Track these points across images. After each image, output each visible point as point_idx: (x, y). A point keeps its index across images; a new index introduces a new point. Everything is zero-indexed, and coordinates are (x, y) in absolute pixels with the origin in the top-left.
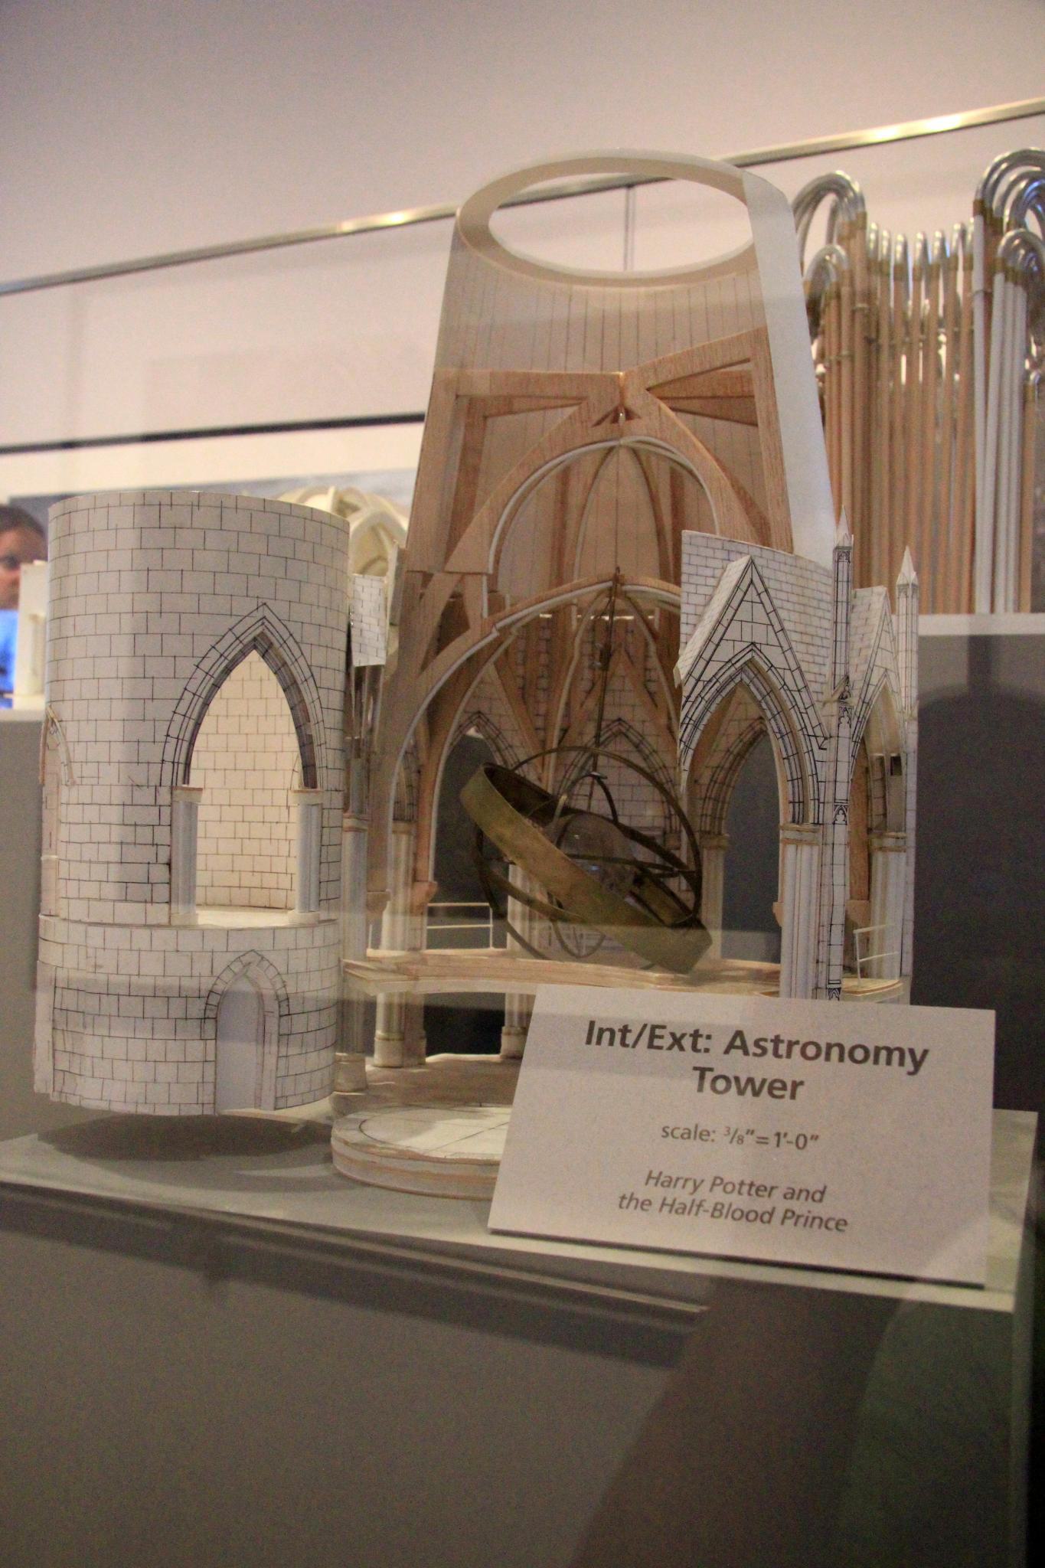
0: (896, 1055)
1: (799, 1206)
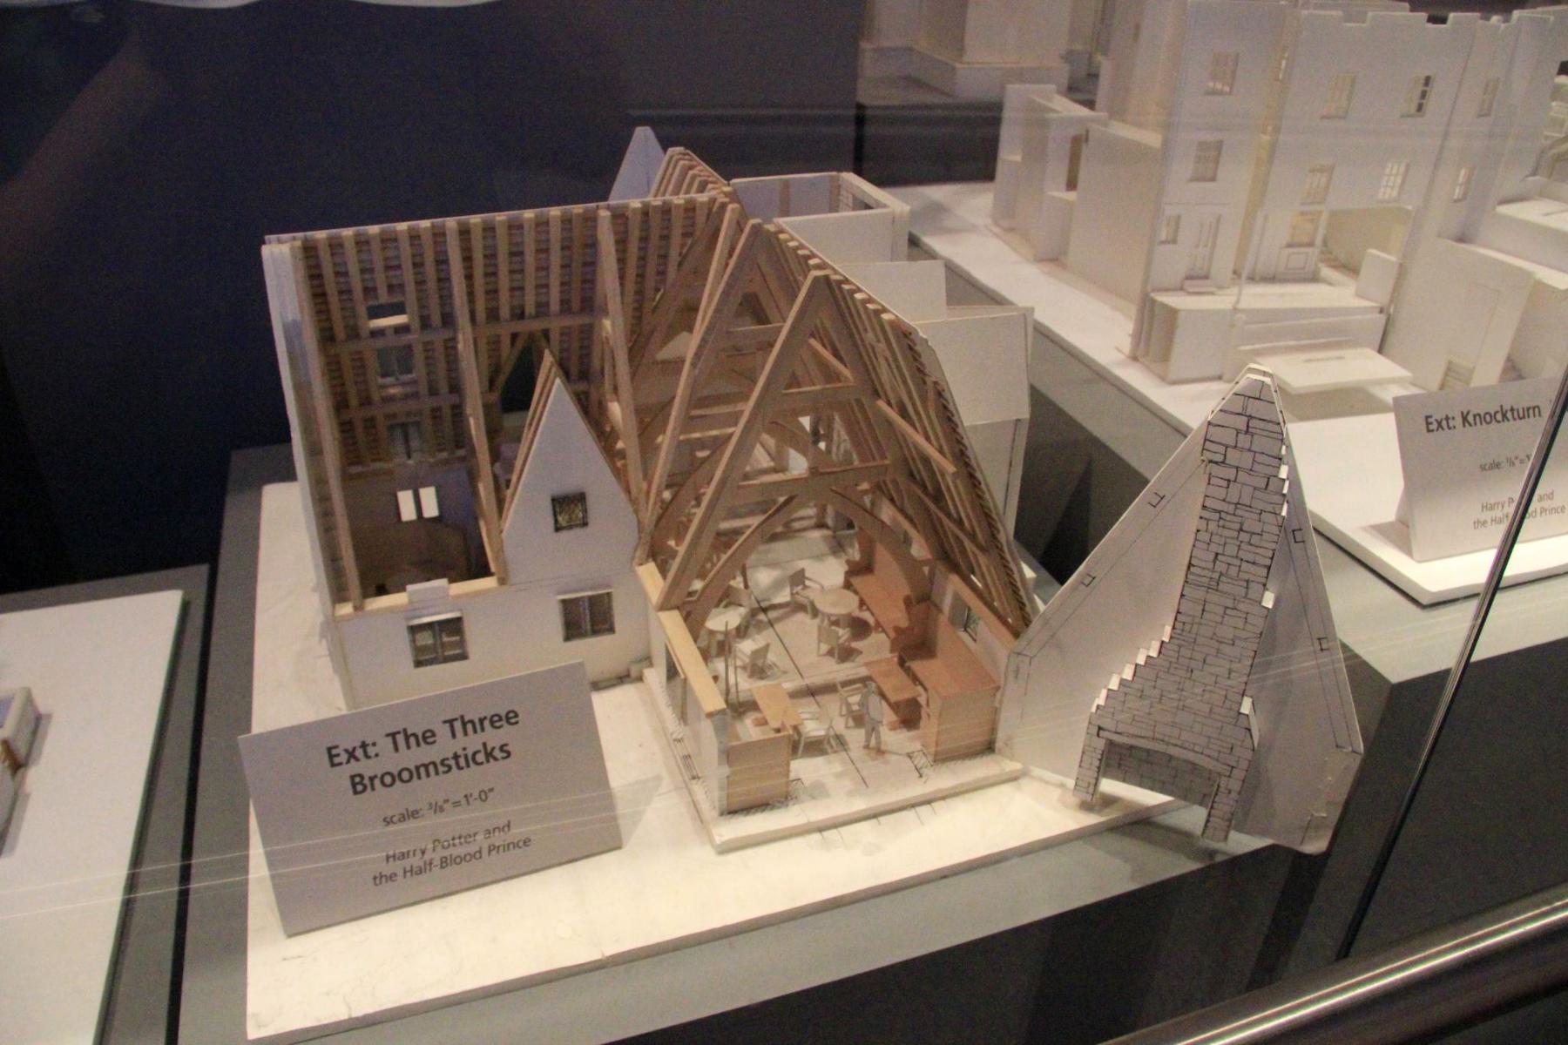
0: (431, 768)
1: (498, 839)
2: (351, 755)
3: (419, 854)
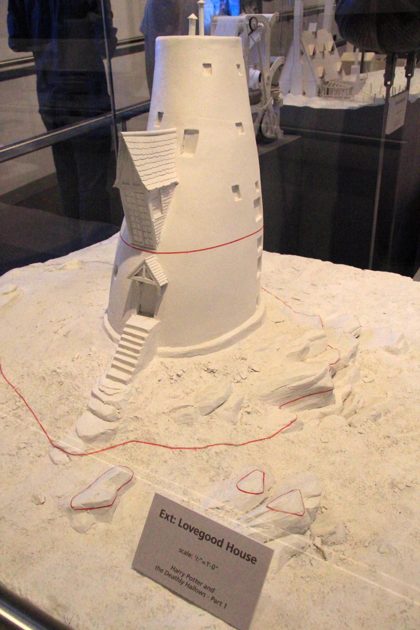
2: (167, 517)
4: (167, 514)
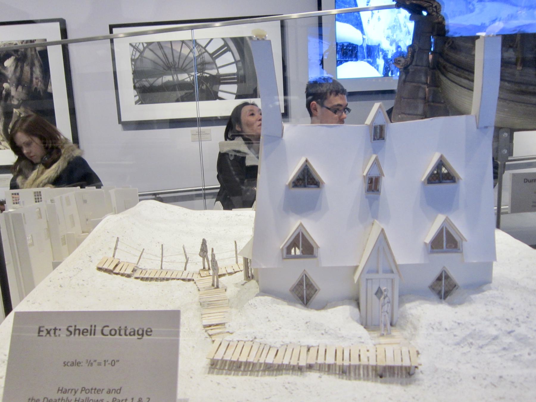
2: (48, 332)
3: (73, 391)
4: (47, 330)
